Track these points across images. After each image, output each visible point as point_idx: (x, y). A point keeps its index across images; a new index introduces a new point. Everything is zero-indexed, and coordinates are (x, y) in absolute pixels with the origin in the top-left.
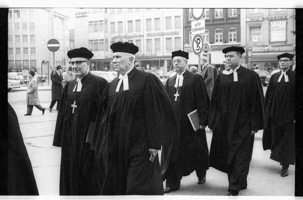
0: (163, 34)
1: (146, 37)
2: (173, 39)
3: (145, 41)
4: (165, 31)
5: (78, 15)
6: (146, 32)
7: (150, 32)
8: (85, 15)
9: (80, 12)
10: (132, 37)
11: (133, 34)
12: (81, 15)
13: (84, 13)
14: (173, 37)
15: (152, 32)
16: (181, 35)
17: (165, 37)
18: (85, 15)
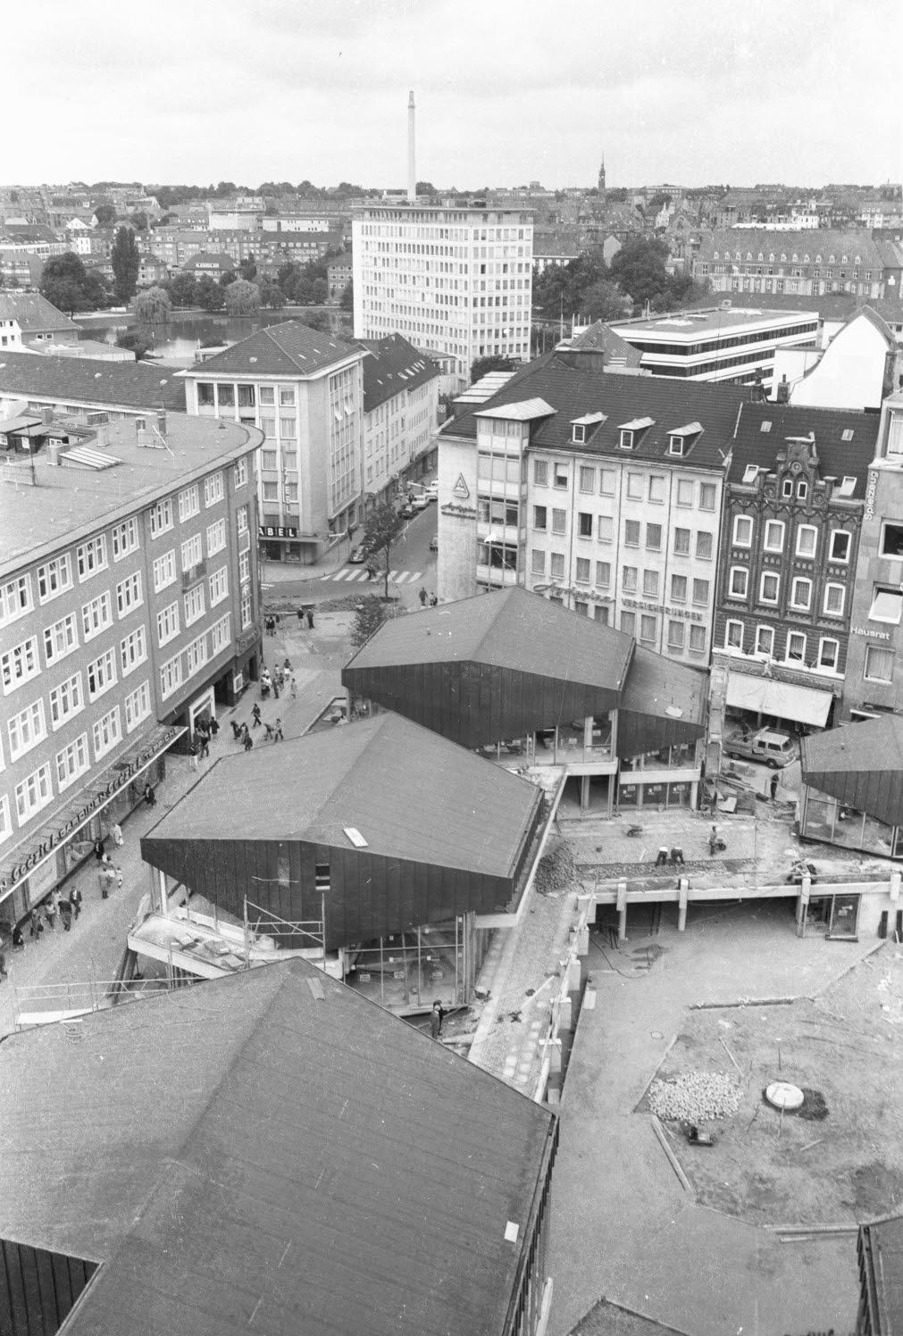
0: (663, 610)
1: (620, 607)
2: (688, 629)
3: (619, 615)
4: (668, 605)
5: (448, 511)
6: (621, 596)
7: (630, 598)
8: (468, 514)
9: (455, 504)
10: (586, 595)
11: (588, 591)
12: (456, 512)
13: (465, 510)
14: (688, 623)
15: (638, 599)
16: (707, 623)
17: (667, 618)
18: (468, 514)
